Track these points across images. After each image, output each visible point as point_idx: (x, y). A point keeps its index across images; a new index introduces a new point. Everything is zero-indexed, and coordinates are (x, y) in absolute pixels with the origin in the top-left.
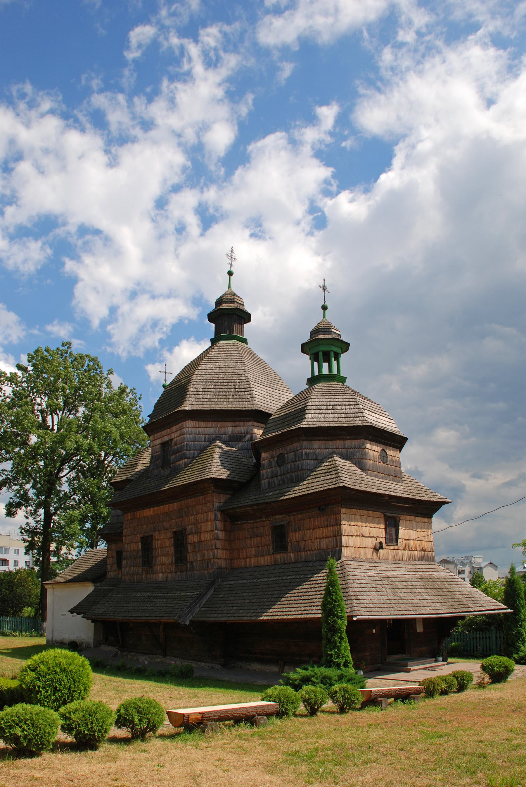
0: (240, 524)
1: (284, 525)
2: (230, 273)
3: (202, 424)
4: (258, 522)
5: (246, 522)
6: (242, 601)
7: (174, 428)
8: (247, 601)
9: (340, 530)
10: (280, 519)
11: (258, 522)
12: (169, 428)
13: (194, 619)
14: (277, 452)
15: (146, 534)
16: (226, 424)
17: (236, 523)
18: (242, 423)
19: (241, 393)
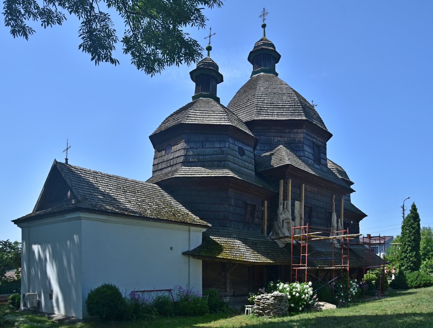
2: (264, 26)
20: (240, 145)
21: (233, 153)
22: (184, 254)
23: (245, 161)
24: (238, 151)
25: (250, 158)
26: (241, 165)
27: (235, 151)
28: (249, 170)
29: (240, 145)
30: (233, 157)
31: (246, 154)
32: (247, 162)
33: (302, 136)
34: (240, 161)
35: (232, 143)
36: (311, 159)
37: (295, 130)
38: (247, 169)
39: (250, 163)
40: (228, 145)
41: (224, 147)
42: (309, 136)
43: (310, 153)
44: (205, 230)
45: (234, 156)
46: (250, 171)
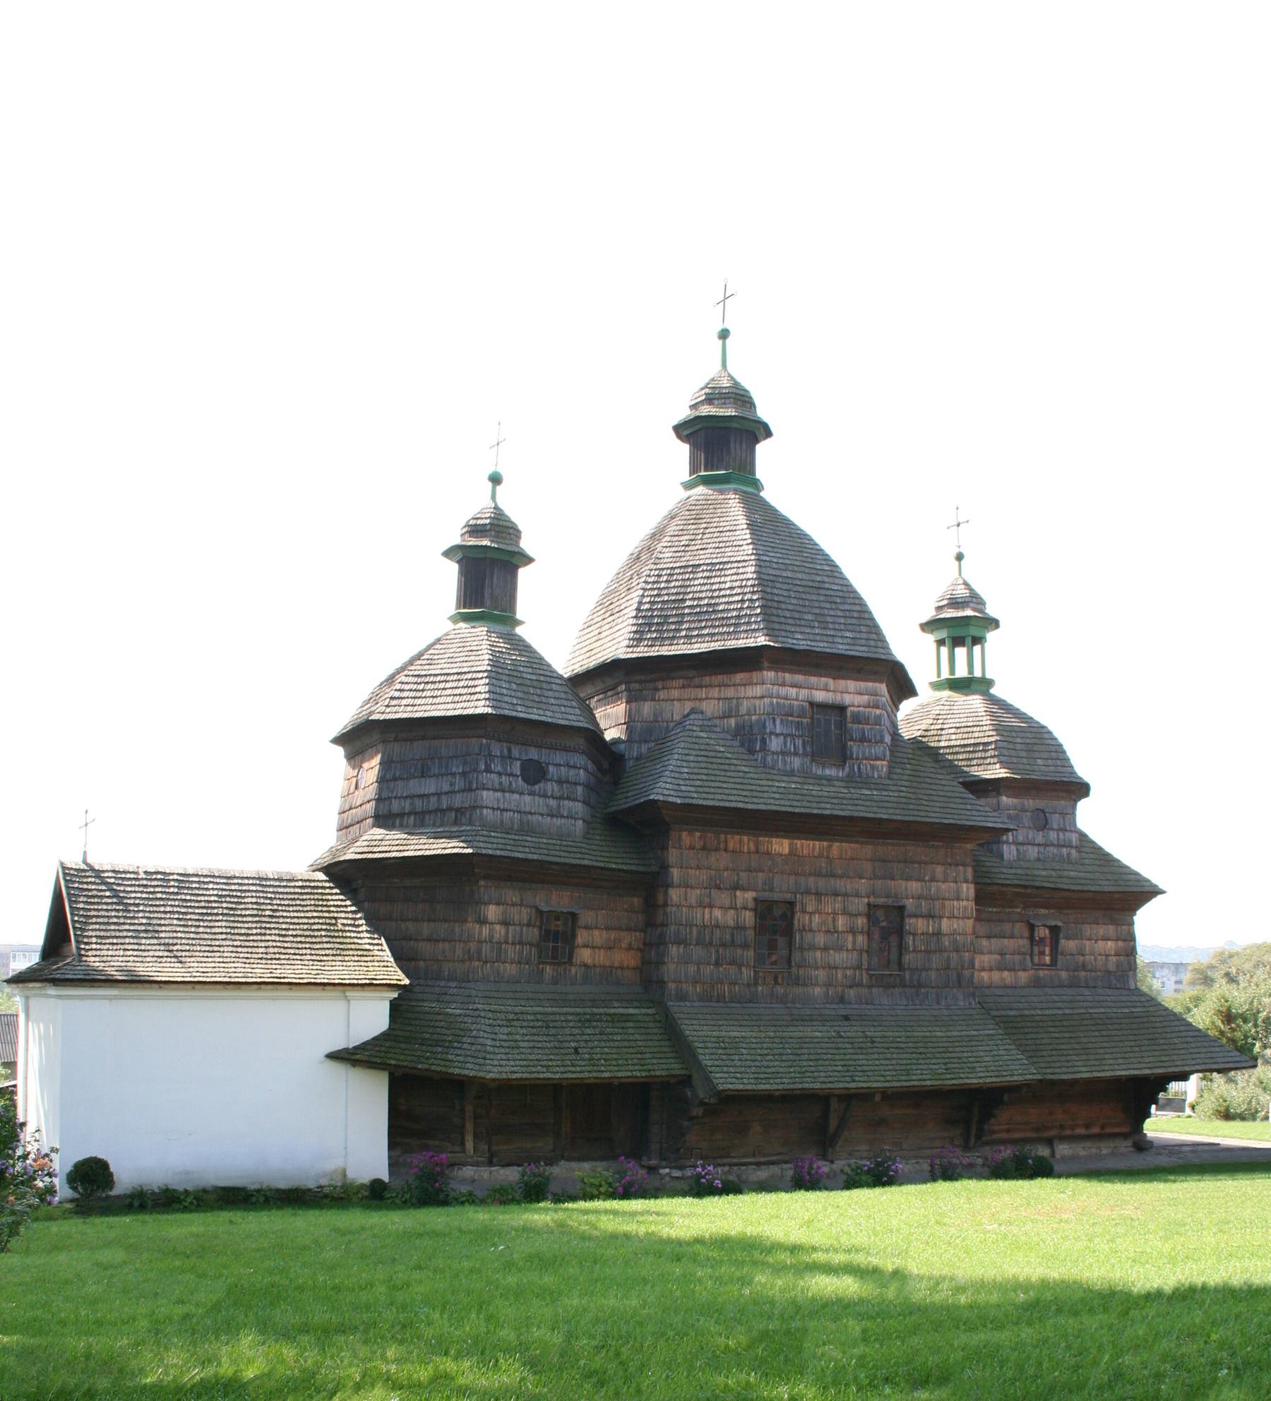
7: (851, 685)
12: (834, 679)
14: (1030, 803)
15: (766, 895)
20: (533, 754)
21: (501, 783)
22: (334, 1056)
23: (545, 796)
24: (518, 773)
25: (567, 782)
26: (528, 809)
27: (511, 775)
28: (562, 816)
29: (533, 754)
30: (499, 794)
31: (550, 776)
32: (553, 797)
33: (758, 690)
34: (527, 799)
35: (502, 757)
36: (796, 754)
37: (739, 677)
38: (552, 816)
39: (564, 799)
40: (486, 763)
41: (475, 770)
42: (791, 686)
43: (791, 735)
44: (395, 995)
45: (503, 791)
46: (563, 821)
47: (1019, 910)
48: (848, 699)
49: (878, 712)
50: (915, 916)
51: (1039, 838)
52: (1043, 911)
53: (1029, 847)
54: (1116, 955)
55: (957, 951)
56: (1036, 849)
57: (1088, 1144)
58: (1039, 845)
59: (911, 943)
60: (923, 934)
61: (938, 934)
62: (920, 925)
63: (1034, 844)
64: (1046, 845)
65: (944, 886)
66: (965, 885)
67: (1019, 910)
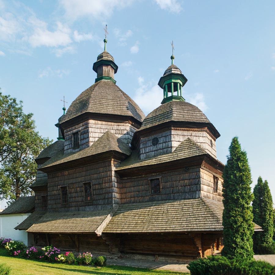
0: (126, 179)
1: (158, 179)
3: (99, 122)
4: (139, 178)
5: (131, 178)
6: (136, 222)
7: (81, 124)
8: (139, 221)
9: (199, 181)
10: (155, 176)
11: (139, 178)
13: (103, 232)
16: (113, 124)
17: (123, 178)
18: (122, 124)
19: (121, 107)
47: (144, 176)
48: (80, 129)
49: (87, 129)
50: (95, 185)
51: (155, 148)
52: (154, 174)
53: (151, 153)
54: (189, 185)
55: (108, 193)
56: (153, 152)
57: (174, 259)
58: (155, 151)
59: (95, 192)
60: (98, 189)
61: (102, 189)
62: (97, 187)
63: (153, 151)
64: (157, 150)
65: (103, 174)
66: (109, 172)
67: (144, 176)
